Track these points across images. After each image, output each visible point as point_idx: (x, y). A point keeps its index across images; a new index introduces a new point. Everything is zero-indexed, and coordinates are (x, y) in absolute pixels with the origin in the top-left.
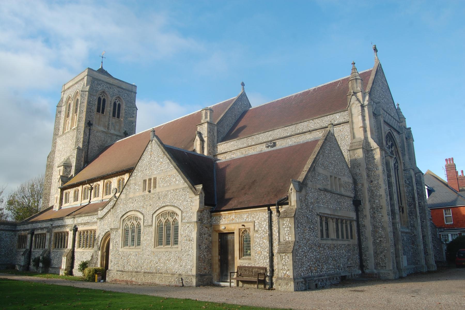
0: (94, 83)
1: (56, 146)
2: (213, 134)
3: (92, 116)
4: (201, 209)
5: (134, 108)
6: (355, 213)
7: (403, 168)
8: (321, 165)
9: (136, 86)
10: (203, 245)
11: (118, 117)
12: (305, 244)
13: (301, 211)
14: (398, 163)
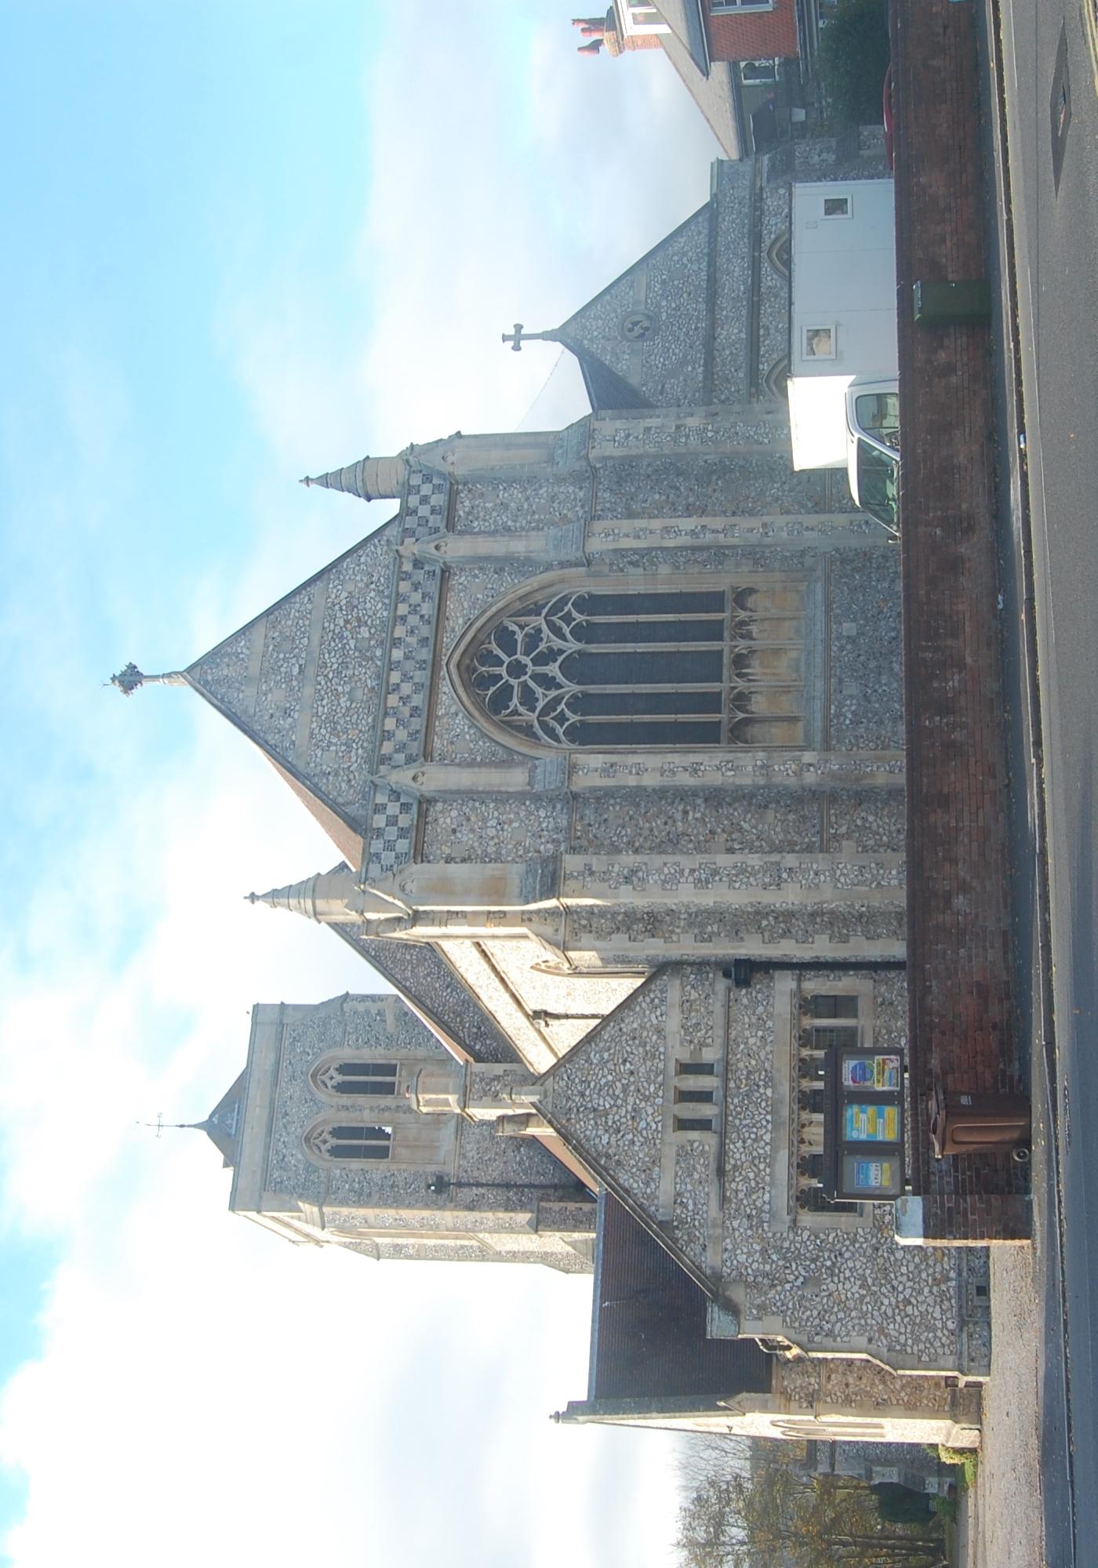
0: (281, 1182)
1: (524, 1253)
2: (497, 1078)
3: (410, 1180)
4: (782, 1406)
5: (343, 1013)
6: (777, 974)
7: (583, 570)
8: (647, 1184)
9: (256, 1007)
10: (875, 1390)
11: (390, 1070)
12: (876, 1302)
13: (789, 1313)
14: (564, 601)
